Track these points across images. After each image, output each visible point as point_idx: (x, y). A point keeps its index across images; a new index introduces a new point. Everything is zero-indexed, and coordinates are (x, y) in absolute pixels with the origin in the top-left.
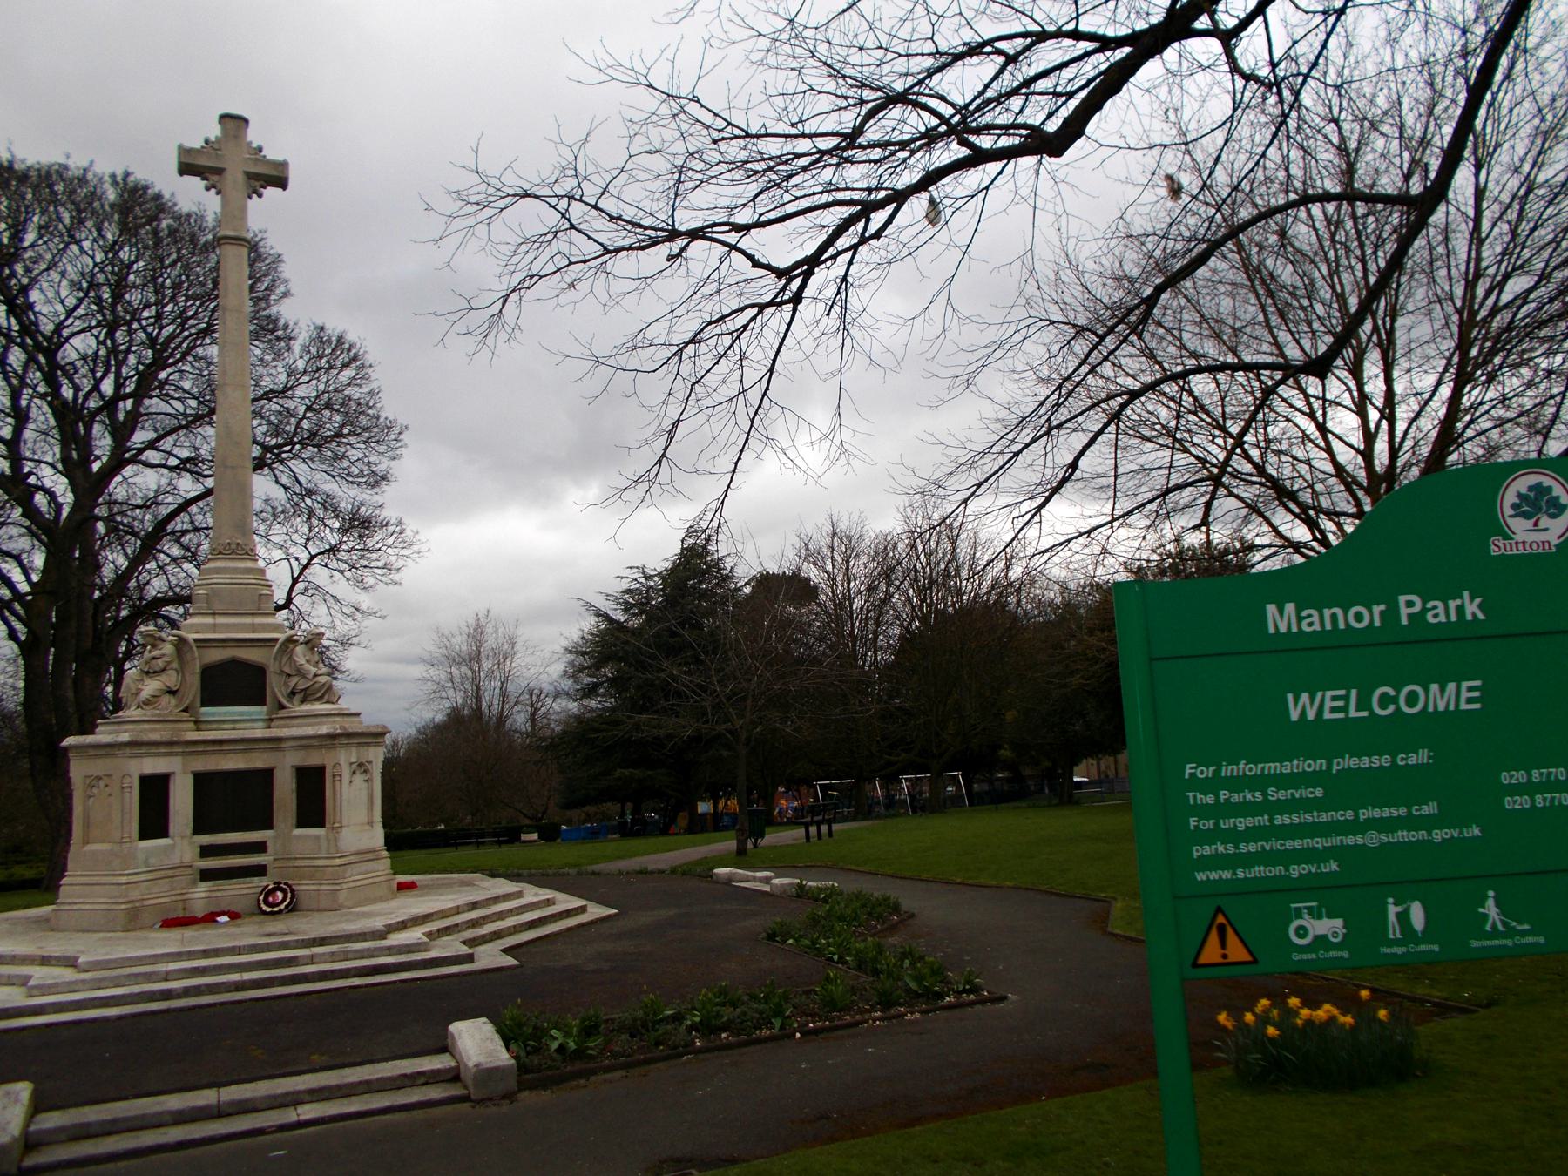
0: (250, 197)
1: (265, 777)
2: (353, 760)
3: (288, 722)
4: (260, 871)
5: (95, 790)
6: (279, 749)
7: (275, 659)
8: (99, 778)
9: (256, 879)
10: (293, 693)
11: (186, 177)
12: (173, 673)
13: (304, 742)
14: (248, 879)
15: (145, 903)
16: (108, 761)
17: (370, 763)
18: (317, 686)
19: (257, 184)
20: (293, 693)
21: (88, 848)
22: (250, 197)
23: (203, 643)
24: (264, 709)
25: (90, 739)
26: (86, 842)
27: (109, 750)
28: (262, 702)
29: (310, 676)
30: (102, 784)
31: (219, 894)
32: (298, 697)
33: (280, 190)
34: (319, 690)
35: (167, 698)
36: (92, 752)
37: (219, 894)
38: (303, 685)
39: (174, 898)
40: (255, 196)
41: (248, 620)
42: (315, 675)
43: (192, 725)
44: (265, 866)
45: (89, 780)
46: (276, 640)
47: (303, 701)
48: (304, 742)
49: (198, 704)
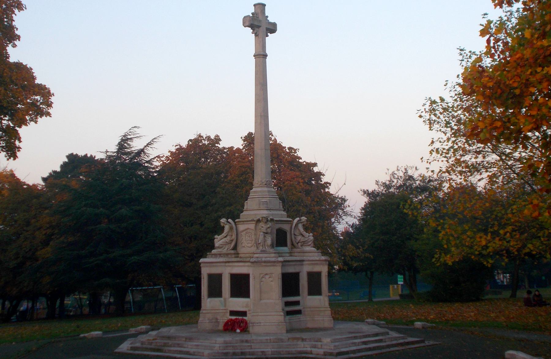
1: (296, 276)
3: (302, 254)
4: (299, 312)
5: (263, 279)
6: (302, 265)
8: (266, 274)
13: (313, 262)
16: (272, 268)
18: (309, 240)
21: (263, 301)
22: (267, 36)
26: (261, 300)
27: (272, 264)
29: (307, 237)
30: (267, 277)
32: (300, 244)
34: (310, 242)
36: (264, 264)
38: (303, 239)
42: (309, 236)
45: (262, 275)
48: (313, 262)
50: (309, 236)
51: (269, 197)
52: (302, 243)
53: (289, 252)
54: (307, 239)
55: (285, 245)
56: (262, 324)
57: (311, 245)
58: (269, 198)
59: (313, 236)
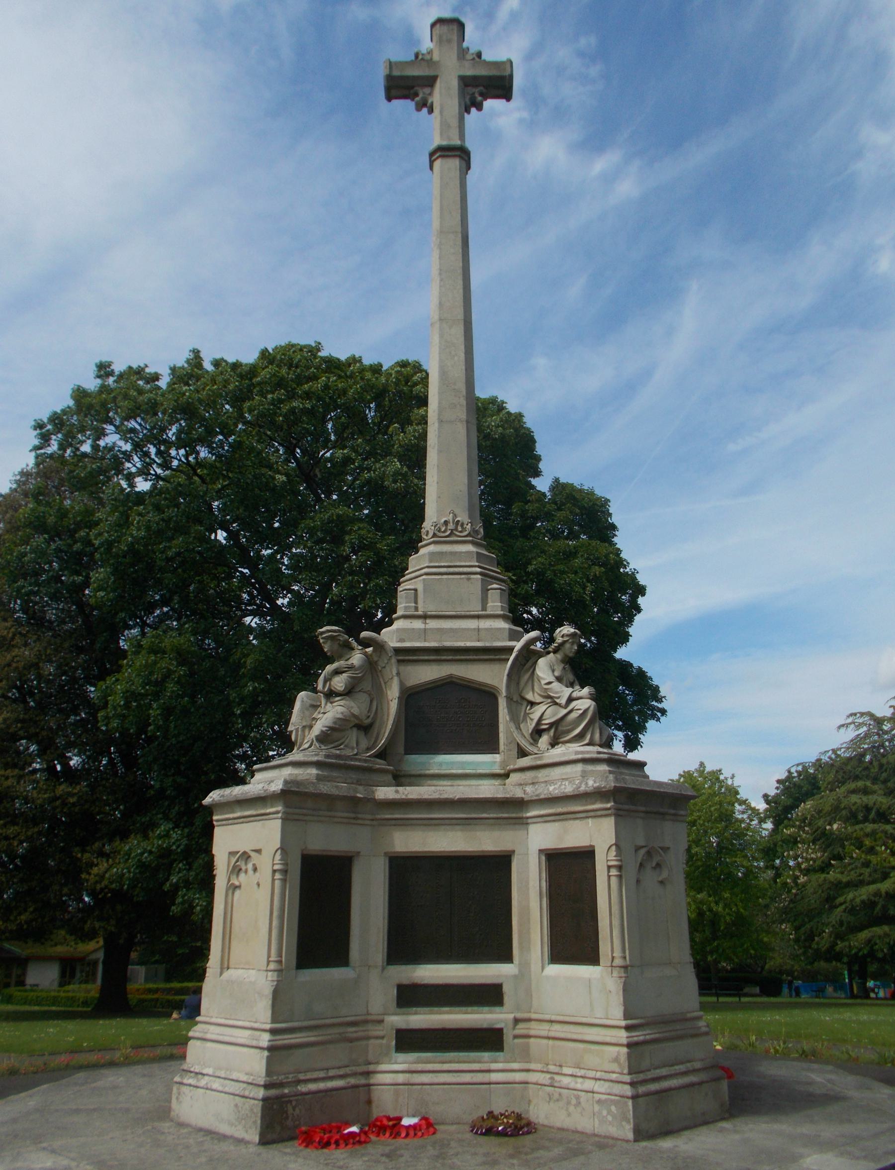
0: (468, 112)
2: (641, 843)
7: (509, 675)
9: (486, 1055)
10: (538, 732)
11: (395, 102)
12: (363, 698)
14: (473, 1055)
15: (303, 1088)
17: (665, 849)
18: (574, 715)
19: (476, 91)
20: (538, 732)
21: (227, 974)
23: (407, 656)
24: (497, 757)
25: (237, 791)
28: (492, 747)
29: (563, 701)
31: (425, 1078)
33: (504, 101)
35: (353, 736)
37: (425, 1078)
38: (552, 715)
39: (352, 1081)
40: (473, 110)
41: (472, 624)
42: (570, 700)
43: (389, 778)
44: (500, 1030)
46: (511, 649)
47: (554, 744)
49: (401, 749)
50: (570, 700)
51: (427, 574)
52: (552, 732)
53: (502, 772)
54: (565, 711)
55: (490, 745)
56: (203, 1082)
57: (588, 737)
58: (424, 577)
59: (592, 697)
